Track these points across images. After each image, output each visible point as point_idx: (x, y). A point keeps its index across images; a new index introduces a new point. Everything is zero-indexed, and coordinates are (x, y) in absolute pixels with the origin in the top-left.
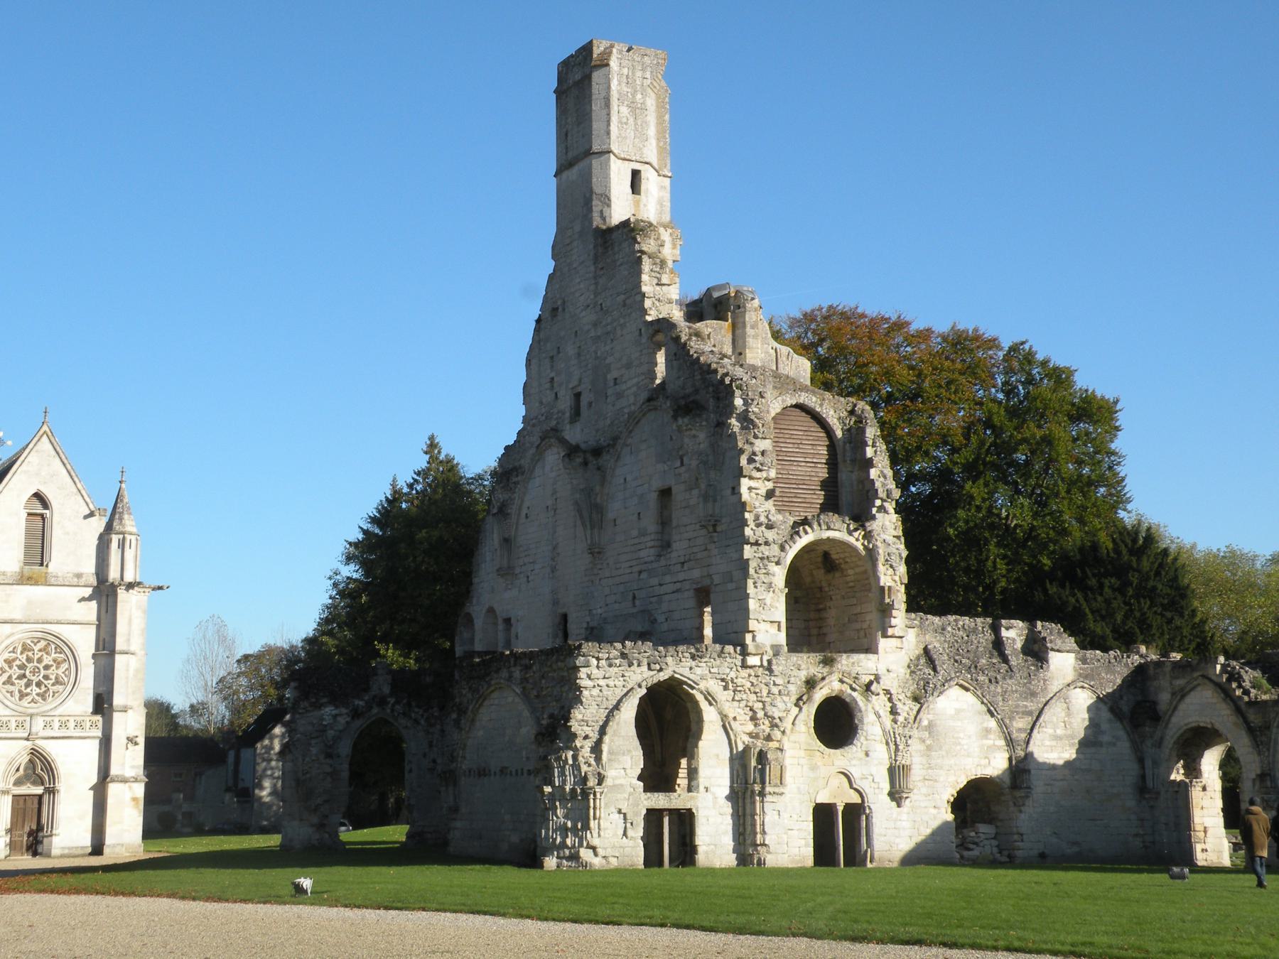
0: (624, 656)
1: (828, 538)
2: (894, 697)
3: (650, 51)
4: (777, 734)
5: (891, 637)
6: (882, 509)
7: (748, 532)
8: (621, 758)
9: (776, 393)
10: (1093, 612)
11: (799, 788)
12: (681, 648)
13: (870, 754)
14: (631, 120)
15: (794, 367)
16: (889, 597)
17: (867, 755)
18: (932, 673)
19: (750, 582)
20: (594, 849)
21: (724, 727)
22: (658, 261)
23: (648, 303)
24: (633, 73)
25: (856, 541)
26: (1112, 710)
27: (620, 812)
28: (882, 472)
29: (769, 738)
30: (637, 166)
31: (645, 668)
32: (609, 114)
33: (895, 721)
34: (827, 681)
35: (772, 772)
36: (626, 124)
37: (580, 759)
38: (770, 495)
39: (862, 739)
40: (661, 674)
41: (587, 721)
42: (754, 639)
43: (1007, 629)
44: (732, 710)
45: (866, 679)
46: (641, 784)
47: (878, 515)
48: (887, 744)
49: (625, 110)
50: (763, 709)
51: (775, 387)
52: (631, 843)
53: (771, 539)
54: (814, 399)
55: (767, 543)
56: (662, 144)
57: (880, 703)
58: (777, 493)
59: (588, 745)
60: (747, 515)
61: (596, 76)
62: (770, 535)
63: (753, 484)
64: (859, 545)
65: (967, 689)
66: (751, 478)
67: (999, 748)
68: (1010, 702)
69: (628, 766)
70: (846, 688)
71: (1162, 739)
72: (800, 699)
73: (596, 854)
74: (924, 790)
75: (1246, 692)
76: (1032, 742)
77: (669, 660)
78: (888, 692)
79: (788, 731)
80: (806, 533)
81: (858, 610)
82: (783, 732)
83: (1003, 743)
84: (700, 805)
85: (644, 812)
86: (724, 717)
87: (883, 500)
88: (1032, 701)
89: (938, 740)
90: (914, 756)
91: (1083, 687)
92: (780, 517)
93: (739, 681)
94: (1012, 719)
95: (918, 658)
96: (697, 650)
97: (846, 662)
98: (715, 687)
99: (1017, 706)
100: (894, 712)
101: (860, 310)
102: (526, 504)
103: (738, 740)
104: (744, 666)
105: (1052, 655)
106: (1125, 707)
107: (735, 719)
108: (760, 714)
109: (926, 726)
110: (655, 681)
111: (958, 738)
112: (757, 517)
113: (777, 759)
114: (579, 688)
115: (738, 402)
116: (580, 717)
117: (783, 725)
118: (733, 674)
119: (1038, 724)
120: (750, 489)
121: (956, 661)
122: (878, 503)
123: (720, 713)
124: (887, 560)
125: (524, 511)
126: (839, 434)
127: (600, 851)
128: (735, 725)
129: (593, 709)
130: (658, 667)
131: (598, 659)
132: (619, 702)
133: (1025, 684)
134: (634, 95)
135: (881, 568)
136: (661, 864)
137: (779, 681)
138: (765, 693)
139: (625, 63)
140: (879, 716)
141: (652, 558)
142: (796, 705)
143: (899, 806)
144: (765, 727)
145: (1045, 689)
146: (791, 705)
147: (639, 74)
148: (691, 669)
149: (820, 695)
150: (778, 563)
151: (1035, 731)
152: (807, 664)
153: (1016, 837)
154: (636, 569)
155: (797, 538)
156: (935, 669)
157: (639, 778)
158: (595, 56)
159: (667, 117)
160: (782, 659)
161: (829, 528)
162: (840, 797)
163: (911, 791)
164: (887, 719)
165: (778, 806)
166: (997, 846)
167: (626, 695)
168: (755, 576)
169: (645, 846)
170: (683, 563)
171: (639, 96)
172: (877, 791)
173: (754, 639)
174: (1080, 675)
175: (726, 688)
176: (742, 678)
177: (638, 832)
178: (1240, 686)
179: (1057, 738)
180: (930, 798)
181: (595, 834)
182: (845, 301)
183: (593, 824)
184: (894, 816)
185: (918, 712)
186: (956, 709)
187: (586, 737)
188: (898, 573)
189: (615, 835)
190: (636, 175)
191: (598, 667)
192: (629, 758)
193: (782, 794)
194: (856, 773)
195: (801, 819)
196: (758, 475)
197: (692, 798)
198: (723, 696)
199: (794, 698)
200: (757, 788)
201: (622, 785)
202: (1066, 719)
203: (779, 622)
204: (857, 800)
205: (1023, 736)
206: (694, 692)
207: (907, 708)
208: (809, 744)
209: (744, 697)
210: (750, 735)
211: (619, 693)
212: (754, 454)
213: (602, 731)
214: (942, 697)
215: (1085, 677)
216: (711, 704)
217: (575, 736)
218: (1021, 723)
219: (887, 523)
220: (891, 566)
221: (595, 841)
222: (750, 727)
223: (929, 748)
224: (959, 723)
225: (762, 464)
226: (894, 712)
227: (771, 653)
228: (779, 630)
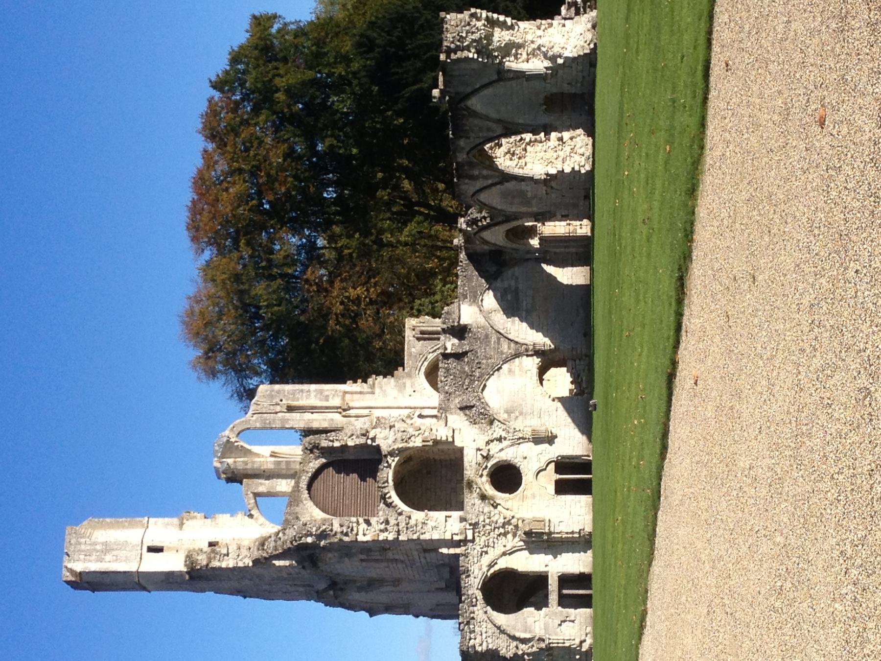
0: (468, 623)
2: (490, 438)
3: (67, 538)
4: (514, 521)
5: (453, 437)
6: (373, 439)
7: (391, 537)
9: (301, 505)
10: (414, 83)
12: (463, 585)
14: (115, 553)
15: (264, 400)
16: (429, 441)
17: (525, 458)
18: (475, 409)
19: (422, 537)
20: (582, 642)
21: (510, 554)
22: (212, 555)
23: (241, 564)
24: (83, 551)
25: (393, 461)
26: (496, 279)
27: (560, 625)
28: (349, 437)
29: (517, 527)
30: (145, 549)
31: (475, 608)
32: (113, 572)
33: (505, 439)
34: (481, 486)
36: (117, 556)
37: (530, 651)
38: (368, 523)
39: (516, 461)
40: (478, 598)
42: (457, 534)
43: (446, 349)
44: (500, 549)
45: (480, 458)
46: (544, 609)
47: (377, 443)
48: (519, 444)
49: (108, 557)
50: (498, 528)
51: (297, 506)
52: (578, 617)
53: (396, 522)
54: (304, 477)
55: (398, 525)
56: (126, 524)
57: (495, 447)
58: (366, 518)
60: (381, 538)
61: (85, 578)
62: (392, 521)
63: (361, 533)
64: (397, 459)
65: (485, 386)
66: (357, 534)
67: (520, 363)
69: (533, 620)
70: (485, 473)
71: (513, 249)
72: (492, 505)
73: (585, 641)
74: (547, 418)
75: (485, 218)
76: (516, 340)
77: (470, 592)
78: (488, 443)
80: (390, 497)
82: (513, 517)
83: (517, 359)
84: (556, 571)
85: (560, 608)
86: (504, 554)
87: (368, 438)
90: (526, 425)
91: (482, 300)
92: (381, 513)
93: (482, 544)
94: (502, 353)
95: (466, 415)
96: (464, 573)
97: (470, 471)
100: (500, 440)
101: (190, 204)
103: (518, 545)
104: (473, 541)
105: (462, 322)
106: (493, 269)
107: (505, 546)
108: (502, 530)
110: (483, 602)
112: (381, 531)
113: (529, 524)
114: (488, 650)
115: (309, 540)
116: (504, 650)
117: (509, 517)
118: (478, 548)
119: (505, 335)
120: (364, 535)
121: (467, 389)
122: (369, 442)
123: (501, 556)
124: (406, 441)
126: (324, 460)
127: (583, 638)
128: (508, 548)
129: (500, 641)
130: (474, 600)
131: (470, 639)
132: (495, 625)
133: (480, 343)
134: (98, 551)
135: (411, 445)
136: (589, 597)
137: (482, 518)
138: (488, 527)
139: (76, 557)
142: (495, 507)
143: (556, 437)
144: (510, 528)
146: (496, 511)
147: (83, 547)
149: (490, 490)
150: (410, 518)
151: (510, 337)
152: (471, 500)
153: (574, 353)
155: (393, 504)
156: (473, 407)
158: (73, 579)
159: (108, 520)
160: (469, 517)
161: (387, 481)
162: (551, 476)
163: (547, 431)
164: (505, 443)
165: (557, 523)
166: (580, 360)
167: (492, 623)
168: (418, 534)
171: (98, 547)
174: (474, 301)
175: (486, 553)
176: (481, 541)
177: (571, 611)
178: (481, 221)
181: (573, 642)
182: (184, 216)
183: (567, 645)
185: (499, 421)
187: (517, 647)
188: (413, 433)
189: (573, 627)
190: (151, 549)
191: (475, 639)
192: (528, 619)
193: (549, 521)
196: (355, 529)
197: (552, 576)
198: (492, 554)
199: (492, 508)
200: (545, 537)
203: (446, 517)
204: (552, 466)
205: (512, 345)
206: (489, 574)
207: (498, 431)
208: (520, 499)
209: (491, 540)
210: (514, 535)
211: (490, 625)
212: (342, 532)
213: (514, 638)
214: (490, 404)
215: (475, 298)
216: (496, 563)
217: (516, 654)
218: (505, 346)
219: (382, 435)
220: (410, 438)
221: (577, 642)
222: (510, 536)
223: (521, 414)
225: (349, 527)
226: (500, 440)
227: (464, 523)
228: (450, 517)
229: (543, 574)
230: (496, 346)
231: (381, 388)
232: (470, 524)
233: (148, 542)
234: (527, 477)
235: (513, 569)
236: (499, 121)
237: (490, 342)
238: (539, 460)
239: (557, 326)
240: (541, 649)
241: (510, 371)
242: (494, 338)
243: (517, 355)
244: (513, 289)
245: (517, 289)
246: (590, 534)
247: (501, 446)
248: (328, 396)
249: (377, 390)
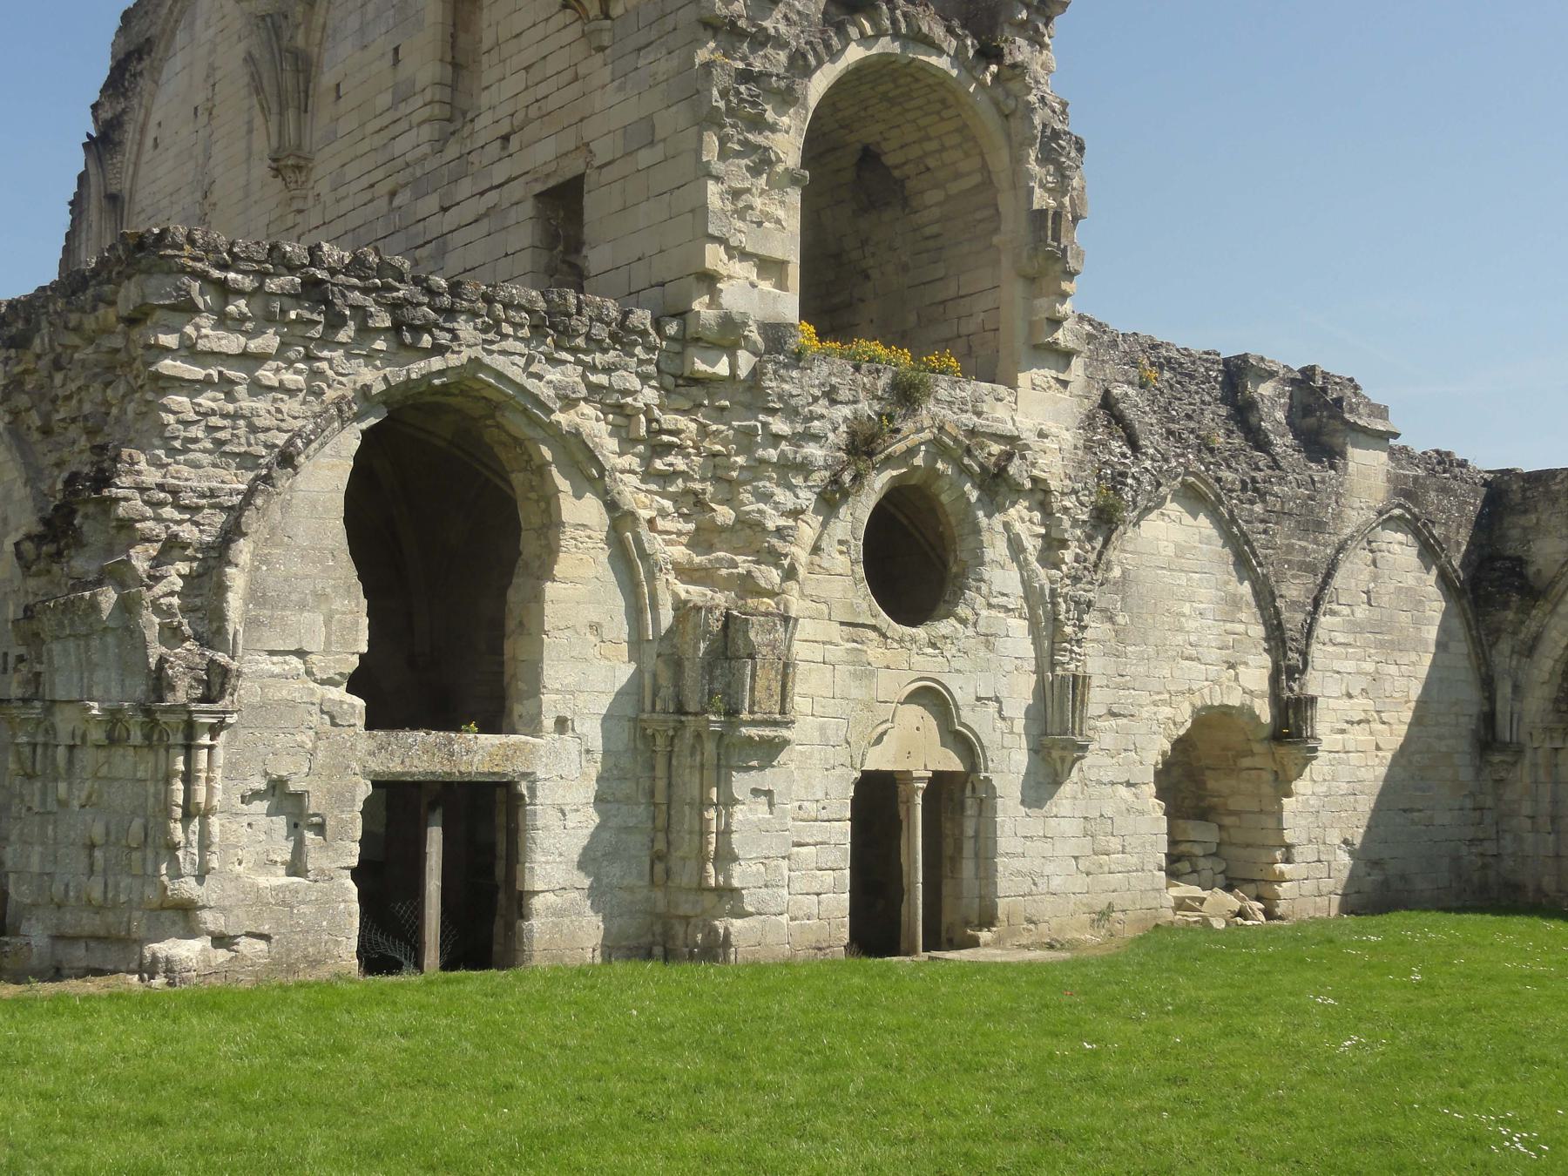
8: (292, 617)
11: (822, 729)
16: (1056, 238)
19: (712, 141)
20: (184, 916)
35: (760, 685)
41: (175, 492)
59: (175, 574)
71: (1537, 638)
72: (835, 480)
79: (802, 572)
81: (952, 291)
82: (790, 574)
85: (364, 789)
86: (619, 517)
98: (591, 422)
99: (1290, 547)
102: (156, 117)
103: (660, 585)
116: (152, 476)
123: (612, 506)
125: (152, 133)
128: (656, 545)
137: (779, 426)
140: (1016, 547)
141: (426, 149)
145: (1338, 516)
148: (530, 360)
149: (879, 482)
154: (383, 189)
156: (1133, 443)
157: (356, 684)
169: (363, 898)
170: (505, 139)
173: (714, 303)
179: (1355, 628)
186: (1177, 545)
194: (962, 691)
195: (824, 814)
201: (292, 705)
202: (1372, 585)
204: (953, 763)
208: (851, 607)
221: (188, 887)
226: (1052, 545)
229: (518, 709)
230: (1296, 558)
232: (756, 373)
235: (551, 552)
240: (159, 682)
243: (1276, 637)
246: (715, 949)
247: (1032, 545)
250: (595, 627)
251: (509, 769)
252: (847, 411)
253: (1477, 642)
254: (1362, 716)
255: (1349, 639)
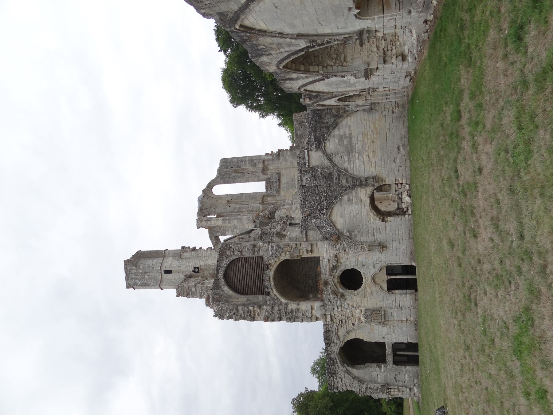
1: (273, 281)
11: (381, 301)
13: (364, 263)
14: (148, 274)
30: (163, 272)
49: (146, 277)
54: (220, 271)
67: (356, 194)
68: (335, 187)
74: (378, 235)
88: (333, 175)
89: (355, 227)
99: (336, 184)
109: (350, 234)
111: (353, 217)
134: (140, 273)
162: (383, 278)
172: (380, 260)
174: (319, 148)
180: (381, 231)
184: (391, 251)
186: (340, 218)
194: (373, 271)
204: (384, 271)
224: (347, 216)
231: (283, 156)
233: (164, 269)
234: (366, 280)
236: (300, 36)
237: (332, 179)
238: (374, 267)
239: (383, 163)
241: (349, 200)
242: (335, 176)
243: (353, 187)
244: (347, 135)
245: (350, 134)
248: (256, 163)
249: (281, 158)
250: (369, 333)
251: (391, 345)
252: (331, 296)
253: (347, 116)
254: (367, 157)
255: (352, 162)
